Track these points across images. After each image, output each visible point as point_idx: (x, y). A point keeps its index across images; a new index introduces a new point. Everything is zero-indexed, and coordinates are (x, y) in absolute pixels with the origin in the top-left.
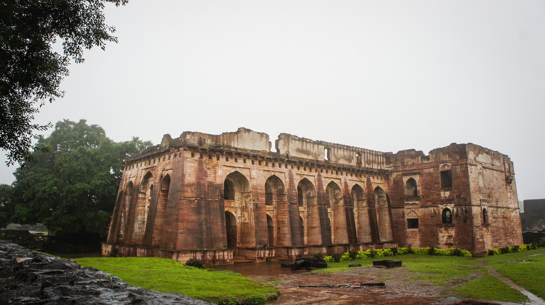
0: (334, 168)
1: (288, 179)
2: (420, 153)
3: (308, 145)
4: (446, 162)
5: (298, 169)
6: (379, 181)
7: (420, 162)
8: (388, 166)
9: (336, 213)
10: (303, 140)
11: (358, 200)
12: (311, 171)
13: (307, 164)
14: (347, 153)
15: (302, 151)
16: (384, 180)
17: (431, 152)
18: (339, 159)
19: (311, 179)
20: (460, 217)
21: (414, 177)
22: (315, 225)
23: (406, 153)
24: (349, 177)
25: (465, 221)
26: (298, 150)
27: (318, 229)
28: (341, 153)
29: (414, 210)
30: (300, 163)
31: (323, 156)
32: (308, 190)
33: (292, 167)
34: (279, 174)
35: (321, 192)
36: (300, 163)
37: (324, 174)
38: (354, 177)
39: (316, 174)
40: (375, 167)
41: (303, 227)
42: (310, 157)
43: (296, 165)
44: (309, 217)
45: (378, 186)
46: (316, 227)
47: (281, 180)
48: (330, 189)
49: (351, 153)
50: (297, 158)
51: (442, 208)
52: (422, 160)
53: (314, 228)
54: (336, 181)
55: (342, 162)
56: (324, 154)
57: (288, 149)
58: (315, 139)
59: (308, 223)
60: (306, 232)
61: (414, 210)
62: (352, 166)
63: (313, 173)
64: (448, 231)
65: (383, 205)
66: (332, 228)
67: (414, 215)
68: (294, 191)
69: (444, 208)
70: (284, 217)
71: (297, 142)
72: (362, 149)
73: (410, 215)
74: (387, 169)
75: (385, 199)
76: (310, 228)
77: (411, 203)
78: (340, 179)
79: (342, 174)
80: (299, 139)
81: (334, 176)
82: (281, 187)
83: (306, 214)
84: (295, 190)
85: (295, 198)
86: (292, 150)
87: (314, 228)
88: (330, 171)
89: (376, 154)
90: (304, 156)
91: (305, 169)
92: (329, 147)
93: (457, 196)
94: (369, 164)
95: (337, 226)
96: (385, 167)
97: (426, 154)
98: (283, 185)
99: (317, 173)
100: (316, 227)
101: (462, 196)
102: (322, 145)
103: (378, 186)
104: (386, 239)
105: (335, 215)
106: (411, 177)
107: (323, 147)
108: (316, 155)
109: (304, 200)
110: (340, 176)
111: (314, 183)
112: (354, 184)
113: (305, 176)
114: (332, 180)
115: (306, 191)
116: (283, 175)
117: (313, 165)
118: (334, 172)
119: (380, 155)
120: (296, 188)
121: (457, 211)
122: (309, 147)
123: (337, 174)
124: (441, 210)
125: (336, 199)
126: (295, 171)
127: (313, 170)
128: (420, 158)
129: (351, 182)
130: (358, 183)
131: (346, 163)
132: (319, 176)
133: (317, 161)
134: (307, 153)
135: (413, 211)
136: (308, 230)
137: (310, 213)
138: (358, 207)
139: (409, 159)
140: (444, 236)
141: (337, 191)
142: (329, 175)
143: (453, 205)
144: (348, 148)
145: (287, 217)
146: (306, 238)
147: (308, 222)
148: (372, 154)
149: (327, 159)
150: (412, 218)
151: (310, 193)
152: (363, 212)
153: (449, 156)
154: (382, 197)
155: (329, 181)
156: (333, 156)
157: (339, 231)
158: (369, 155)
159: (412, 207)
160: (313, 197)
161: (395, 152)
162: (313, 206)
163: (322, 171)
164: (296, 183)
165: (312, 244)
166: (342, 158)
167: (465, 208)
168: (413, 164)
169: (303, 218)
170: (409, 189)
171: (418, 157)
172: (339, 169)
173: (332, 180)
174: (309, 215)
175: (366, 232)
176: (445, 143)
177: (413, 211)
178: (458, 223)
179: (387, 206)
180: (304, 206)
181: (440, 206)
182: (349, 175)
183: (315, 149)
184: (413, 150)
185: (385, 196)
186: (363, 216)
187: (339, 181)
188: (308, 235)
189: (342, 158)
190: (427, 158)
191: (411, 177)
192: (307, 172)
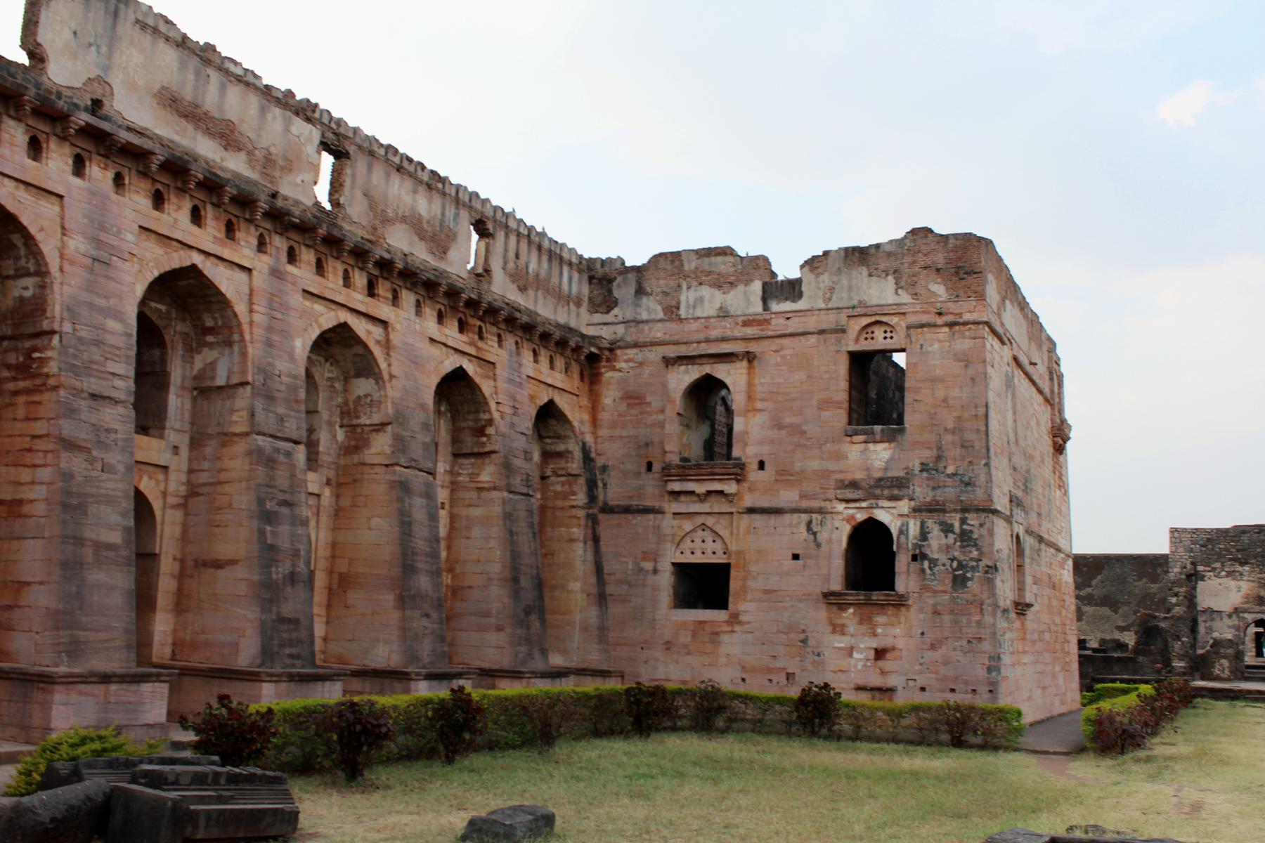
0: (360, 254)
1: (77, 244)
2: (760, 264)
3: (234, 93)
4: (884, 310)
5: (158, 200)
6: (558, 378)
7: (758, 307)
8: (598, 318)
9: (345, 502)
10: (206, 55)
11: (456, 455)
12: (230, 230)
13: (212, 186)
14: (425, 206)
15: (192, 114)
16: (576, 376)
17: (812, 264)
18: (386, 221)
19: (226, 281)
20: (933, 562)
21: (721, 371)
22: (223, 550)
23: (690, 265)
24: (430, 325)
25: (959, 581)
26: (171, 102)
27: (240, 572)
28: (399, 192)
29: (710, 521)
30: (172, 175)
31: (308, 177)
32: (203, 344)
33: (118, 180)
34: (22, 194)
35: (281, 365)
36: (172, 175)
37: (303, 273)
38: (451, 333)
39: (261, 264)
40: (546, 311)
41: (154, 557)
42: (234, 164)
43: (145, 174)
44: (198, 504)
45: (551, 402)
46: (233, 562)
47: (28, 238)
48: (325, 373)
49: (450, 212)
50: (160, 140)
51: (850, 519)
52: (765, 300)
53: (218, 565)
54: (360, 327)
55: (400, 242)
56: (316, 168)
57: (107, 69)
58: (272, 77)
59: (184, 538)
60: (166, 585)
61: (710, 521)
62: (443, 273)
63: (244, 251)
64: (873, 627)
65: (565, 496)
66: (320, 580)
67: (710, 545)
68: (112, 324)
69: (861, 517)
70: (25, 475)
71: (169, 56)
72: (496, 208)
73: (687, 544)
74: (591, 331)
75: (575, 466)
76: (199, 564)
77: (701, 488)
78: (384, 324)
79: (395, 300)
80: (183, 43)
81: (358, 298)
82: (25, 287)
83: (176, 483)
84: (117, 315)
85: (121, 368)
86: (132, 87)
87: (218, 565)
88: (340, 267)
89: (555, 254)
90: (206, 149)
91: (197, 217)
92: (340, 142)
93: (924, 467)
94: (522, 289)
95: (344, 569)
96: (586, 322)
97: (786, 269)
98: (41, 272)
99: (264, 258)
100: (233, 562)
101: (950, 470)
102: (309, 120)
103: (551, 402)
104: (564, 652)
105: (338, 513)
106: (707, 369)
107: (315, 134)
108: (269, 161)
109: (177, 403)
110: (383, 310)
111: (240, 308)
112: (450, 363)
113: (197, 259)
114: (344, 316)
115: (191, 351)
116: (49, 209)
117: (245, 202)
118: (360, 279)
119: (570, 264)
120: (132, 312)
121: (924, 535)
122: (236, 106)
123: (371, 291)
124: (847, 529)
125: (351, 428)
126: (135, 204)
127: (247, 238)
128: (757, 286)
129: (436, 351)
130: (470, 368)
131: (421, 254)
132: (276, 273)
133: (274, 195)
134: (228, 136)
135: (704, 526)
136: (182, 576)
137: (203, 478)
138: (454, 487)
139: (706, 291)
140: (850, 651)
141: (362, 386)
142: (332, 284)
143: (904, 506)
144: (435, 183)
145: (45, 474)
146: (162, 625)
147: (185, 528)
148: (540, 248)
149: (328, 207)
150: (698, 558)
151: (213, 365)
152: (476, 512)
153: (898, 286)
154: (560, 455)
155: (329, 319)
156: (359, 194)
157: (353, 596)
158: (524, 245)
159: (705, 507)
160: (230, 388)
161: (636, 258)
162: (227, 438)
163: (292, 257)
164: (132, 284)
165: (198, 660)
166: (404, 219)
167: (963, 521)
168: (724, 314)
169: (157, 505)
170: (687, 426)
171: (748, 282)
172: (385, 266)
173: (344, 316)
174: (193, 491)
175: (487, 614)
176: (882, 229)
177: (704, 526)
178: (925, 588)
179: (581, 498)
180: (172, 436)
181: (840, 507)
182: (430, 313)
183: (275, 131)
184: (726, 252)
185: (578, 454)
186: (477, 532)
187: (377, 331)
188: (181, 604)
189: (404, 219)
190: (792, 289)
191: (707, 369)
192: (209, 236)
